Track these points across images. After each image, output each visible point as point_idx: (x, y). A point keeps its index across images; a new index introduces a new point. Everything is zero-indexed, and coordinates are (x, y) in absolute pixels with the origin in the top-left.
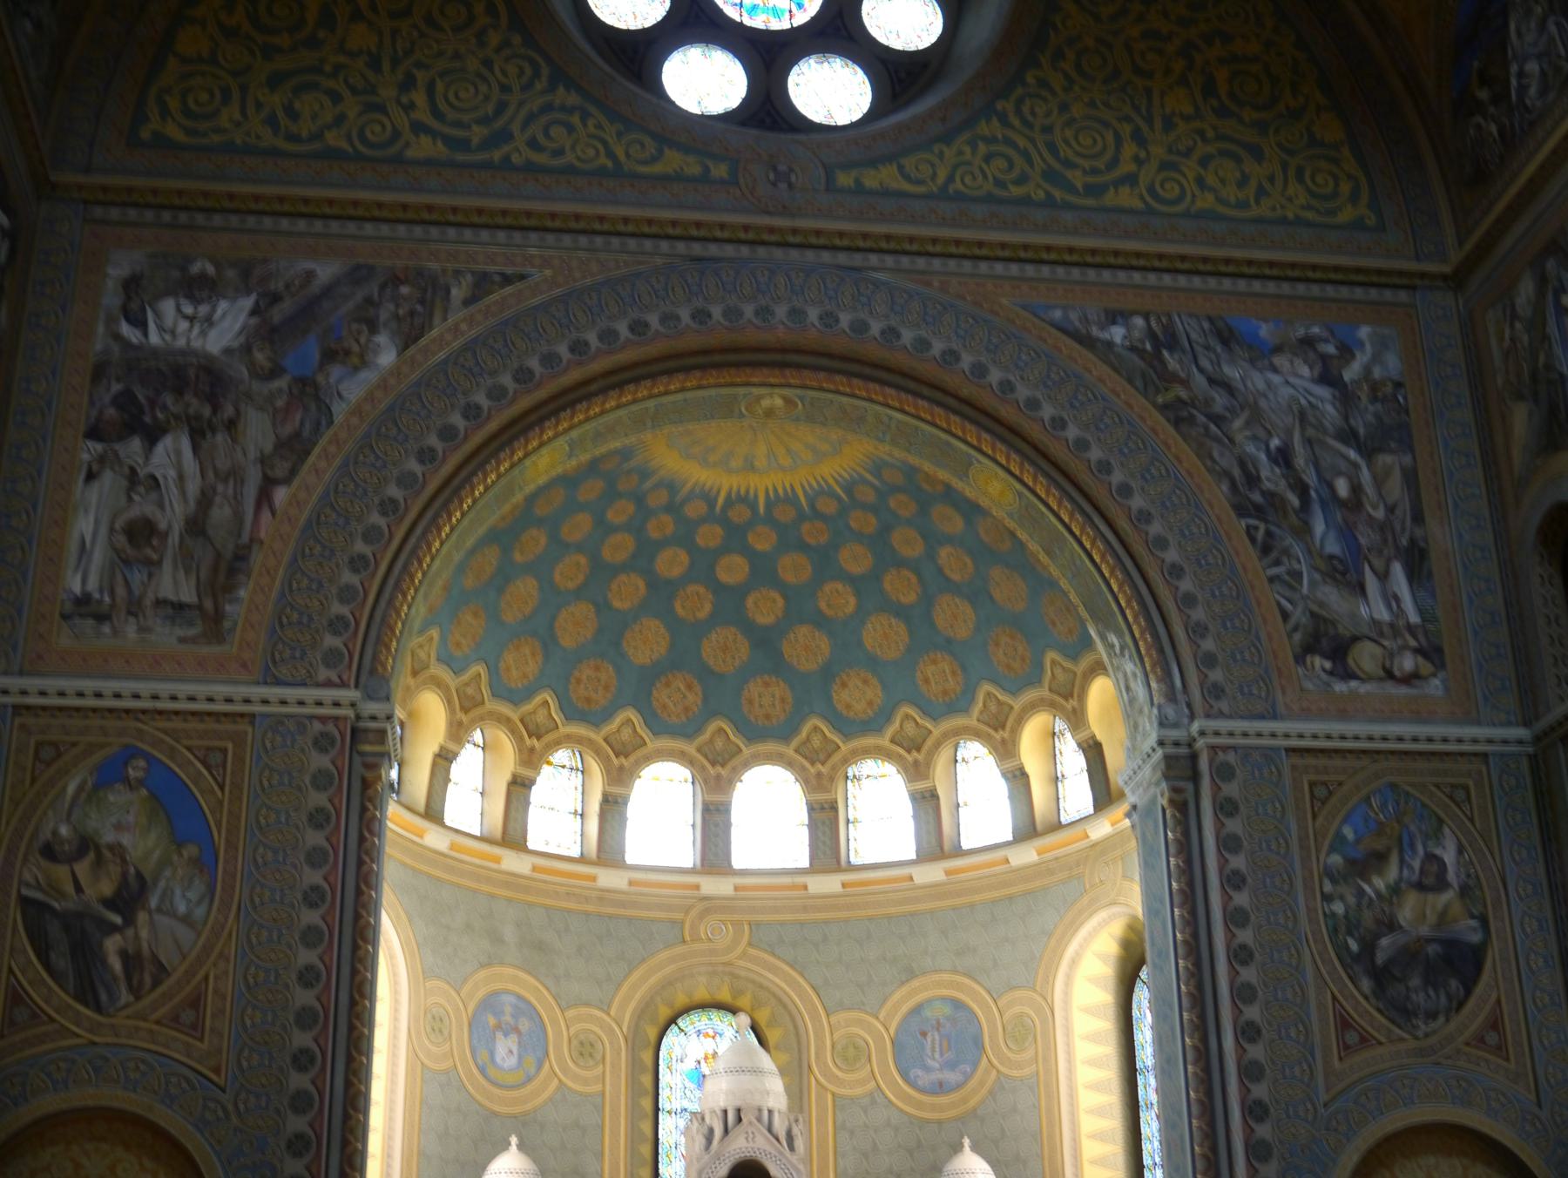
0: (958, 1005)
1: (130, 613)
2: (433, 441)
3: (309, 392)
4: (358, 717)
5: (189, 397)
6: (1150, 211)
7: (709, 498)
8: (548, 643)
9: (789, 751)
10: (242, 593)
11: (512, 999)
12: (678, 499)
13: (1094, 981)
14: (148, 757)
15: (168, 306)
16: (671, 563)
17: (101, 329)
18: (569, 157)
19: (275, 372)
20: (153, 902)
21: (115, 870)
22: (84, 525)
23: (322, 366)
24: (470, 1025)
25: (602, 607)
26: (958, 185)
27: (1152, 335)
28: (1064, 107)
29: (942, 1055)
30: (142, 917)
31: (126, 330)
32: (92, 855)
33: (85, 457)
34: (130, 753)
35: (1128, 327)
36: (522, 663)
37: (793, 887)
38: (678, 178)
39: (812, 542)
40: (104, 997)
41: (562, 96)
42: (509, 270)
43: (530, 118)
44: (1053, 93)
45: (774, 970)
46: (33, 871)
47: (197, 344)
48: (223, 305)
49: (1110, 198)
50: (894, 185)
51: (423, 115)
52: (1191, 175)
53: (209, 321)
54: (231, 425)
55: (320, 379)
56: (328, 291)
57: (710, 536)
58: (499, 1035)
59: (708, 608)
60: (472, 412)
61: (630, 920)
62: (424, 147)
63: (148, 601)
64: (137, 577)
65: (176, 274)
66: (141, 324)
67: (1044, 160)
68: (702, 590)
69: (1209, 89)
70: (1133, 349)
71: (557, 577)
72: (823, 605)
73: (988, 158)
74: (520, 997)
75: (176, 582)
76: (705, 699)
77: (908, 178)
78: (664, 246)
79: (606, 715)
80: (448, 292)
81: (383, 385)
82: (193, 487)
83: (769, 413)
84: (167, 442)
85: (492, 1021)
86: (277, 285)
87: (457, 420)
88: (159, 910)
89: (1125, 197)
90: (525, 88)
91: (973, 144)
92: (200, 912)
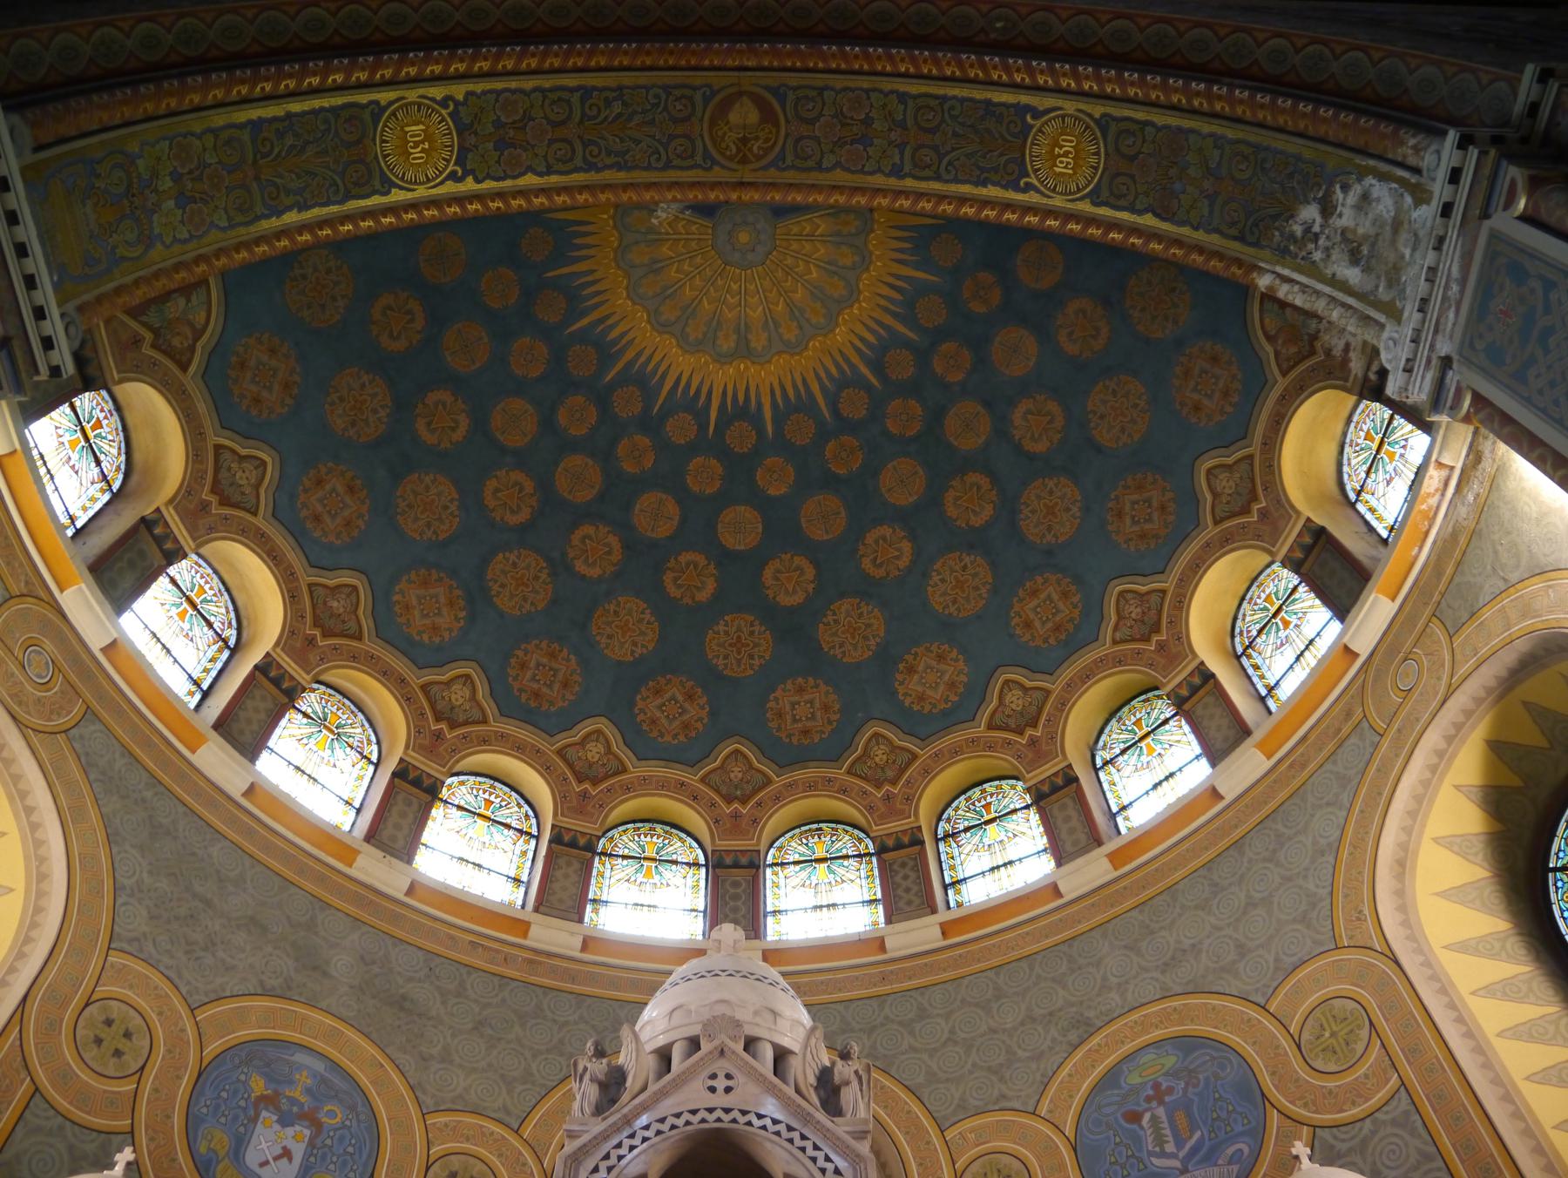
0: (1187, 1044)
7: (694, 405)
8: (477, 597)
11: (319, 1066)
13: (1452, 894)
29: (1179, 1144)
59: (711, 585)
72: (867, 564)
74: (335, 1066)
76: (713, 714)
85: (258, 1086)
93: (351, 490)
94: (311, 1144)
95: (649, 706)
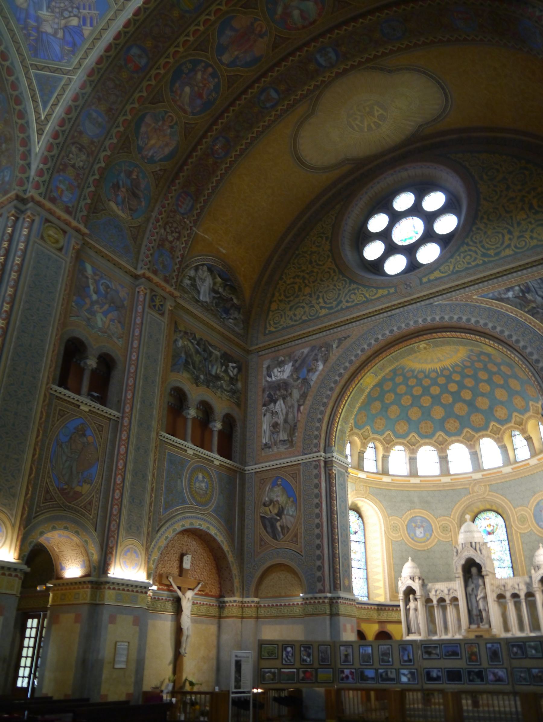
1: (275, 445)
2: (333, 385)
3: (306, 381)
4: (326, 459)
5: (282, 391)
6: (516, 253)
7: (435, 371)
8: (409, 420)
9: (488, 433)
10: (296, 434)
11: (420, 518)
12: (427, 374)
14: (281, 478)
15: (275, 370)
16: (436, 390)
17: (263, 380)
18: (356, 302)
19: (298, 379)
20: (285, 513)
21: (277, 506)
22: (264, 427)
23: (307, 374)
24: (407, 527)
25: (421, 407)
26: (457, 269)
27: (522, 291)
28: (485, 233)
30: (283, 517)
31: (269, 379)
32: (272, 504)
33: (263, 411)
34: (278, 478)
35: (514, 291)
36: (402, 427)
37: (498, 472)
38: (383, 296)
39: (470, 374)
40: (278, 537)
41: (354, 286)
42: (345, 336)
43: (346, 294)
44: (481, 230)
45: (497, 497)
46: (262, 509)
47: (282, 378)
48: (286, 366)
49: (503, 254)
50: (438, 276)
51: (322, 304)
52: (528, 237)
53: (284, 371)
54: (291, 394)
55: (307, 377)
56: (307, 355)
57: (442, 381)
58: (417, 528)
60: (340, 375)
61: (453, 490)
62: (324, 312)
63: (278, 442)
64: (275, 436)
65: (276, 362)
66: (270, 376)
67: (481, 251)
68: (447, 395)
69: (531, 207)
70: (516, 297)
71: (403, 403)
72: (481, 390)
73: (464, 258)
75: (283, 436)
76: (460, 424)
77: (442, 273)
78: (381, 316)
79: (433, 434)
80: (332, 346)
81: (320, 374)
82: (284, 412)
83: (425, 348)
84: (278, 403)
85: (414, 525)
86: (296, 358)
87: (337, 378)
88: (287, 515)
89: (508, 252)
90: (344, 288)
91: (459, 255)
92: (295, 514)
93: (381, 419)
94: (424, 530)
95: (447, 426)
